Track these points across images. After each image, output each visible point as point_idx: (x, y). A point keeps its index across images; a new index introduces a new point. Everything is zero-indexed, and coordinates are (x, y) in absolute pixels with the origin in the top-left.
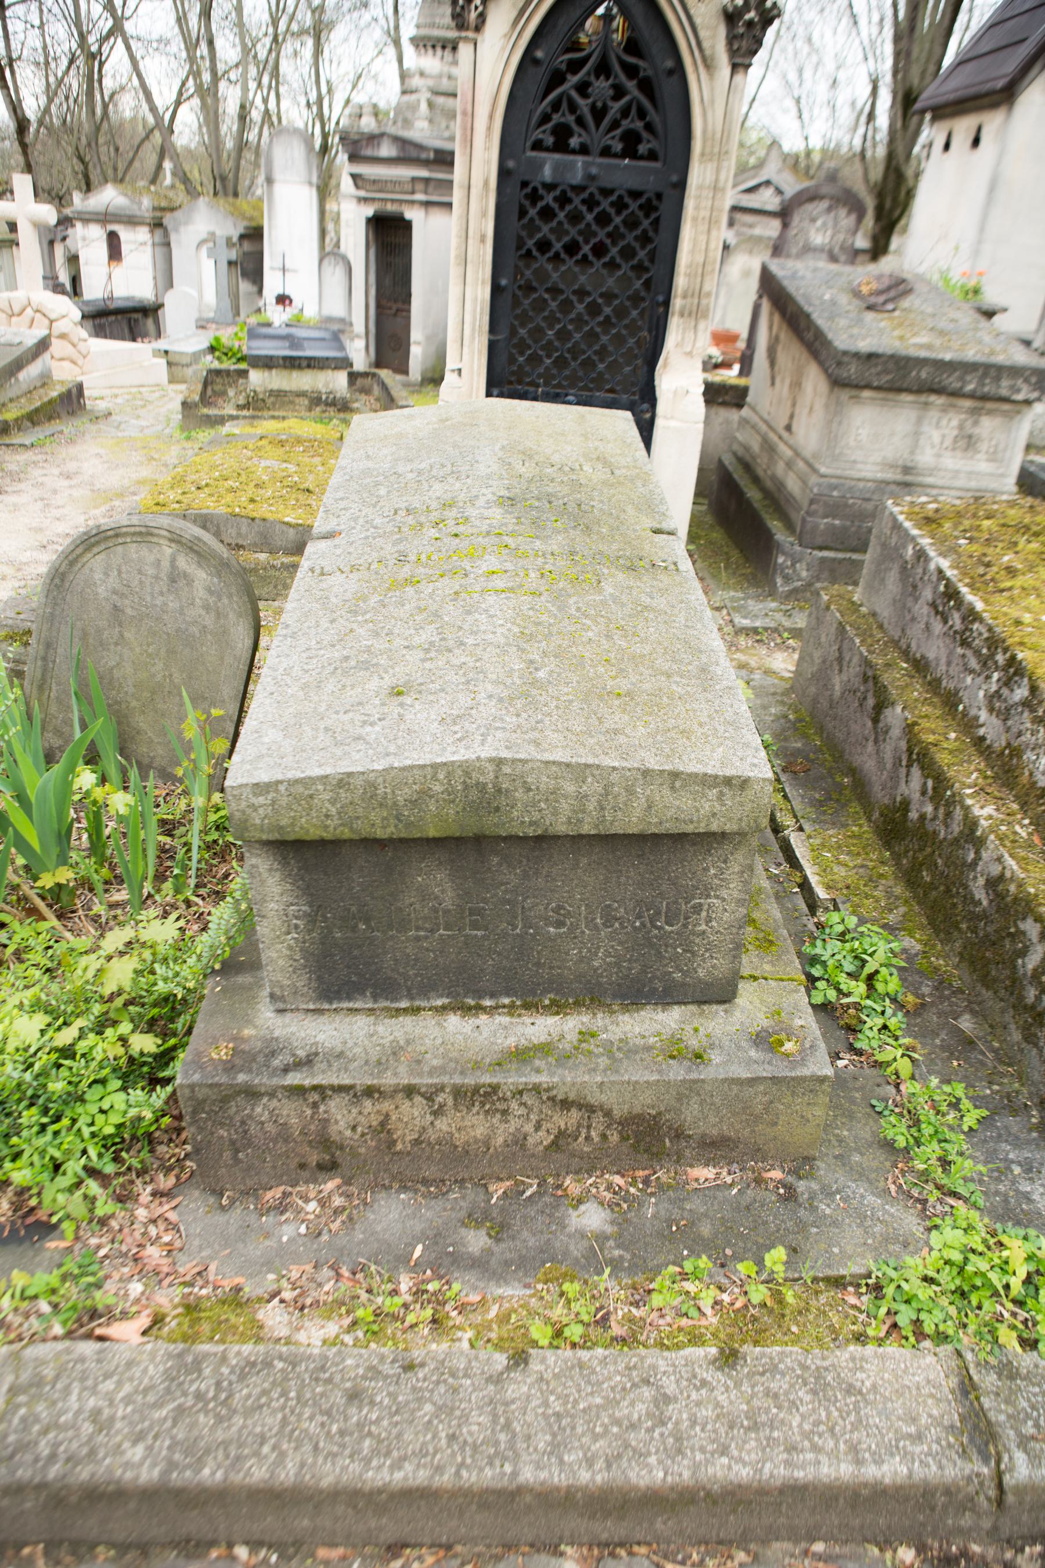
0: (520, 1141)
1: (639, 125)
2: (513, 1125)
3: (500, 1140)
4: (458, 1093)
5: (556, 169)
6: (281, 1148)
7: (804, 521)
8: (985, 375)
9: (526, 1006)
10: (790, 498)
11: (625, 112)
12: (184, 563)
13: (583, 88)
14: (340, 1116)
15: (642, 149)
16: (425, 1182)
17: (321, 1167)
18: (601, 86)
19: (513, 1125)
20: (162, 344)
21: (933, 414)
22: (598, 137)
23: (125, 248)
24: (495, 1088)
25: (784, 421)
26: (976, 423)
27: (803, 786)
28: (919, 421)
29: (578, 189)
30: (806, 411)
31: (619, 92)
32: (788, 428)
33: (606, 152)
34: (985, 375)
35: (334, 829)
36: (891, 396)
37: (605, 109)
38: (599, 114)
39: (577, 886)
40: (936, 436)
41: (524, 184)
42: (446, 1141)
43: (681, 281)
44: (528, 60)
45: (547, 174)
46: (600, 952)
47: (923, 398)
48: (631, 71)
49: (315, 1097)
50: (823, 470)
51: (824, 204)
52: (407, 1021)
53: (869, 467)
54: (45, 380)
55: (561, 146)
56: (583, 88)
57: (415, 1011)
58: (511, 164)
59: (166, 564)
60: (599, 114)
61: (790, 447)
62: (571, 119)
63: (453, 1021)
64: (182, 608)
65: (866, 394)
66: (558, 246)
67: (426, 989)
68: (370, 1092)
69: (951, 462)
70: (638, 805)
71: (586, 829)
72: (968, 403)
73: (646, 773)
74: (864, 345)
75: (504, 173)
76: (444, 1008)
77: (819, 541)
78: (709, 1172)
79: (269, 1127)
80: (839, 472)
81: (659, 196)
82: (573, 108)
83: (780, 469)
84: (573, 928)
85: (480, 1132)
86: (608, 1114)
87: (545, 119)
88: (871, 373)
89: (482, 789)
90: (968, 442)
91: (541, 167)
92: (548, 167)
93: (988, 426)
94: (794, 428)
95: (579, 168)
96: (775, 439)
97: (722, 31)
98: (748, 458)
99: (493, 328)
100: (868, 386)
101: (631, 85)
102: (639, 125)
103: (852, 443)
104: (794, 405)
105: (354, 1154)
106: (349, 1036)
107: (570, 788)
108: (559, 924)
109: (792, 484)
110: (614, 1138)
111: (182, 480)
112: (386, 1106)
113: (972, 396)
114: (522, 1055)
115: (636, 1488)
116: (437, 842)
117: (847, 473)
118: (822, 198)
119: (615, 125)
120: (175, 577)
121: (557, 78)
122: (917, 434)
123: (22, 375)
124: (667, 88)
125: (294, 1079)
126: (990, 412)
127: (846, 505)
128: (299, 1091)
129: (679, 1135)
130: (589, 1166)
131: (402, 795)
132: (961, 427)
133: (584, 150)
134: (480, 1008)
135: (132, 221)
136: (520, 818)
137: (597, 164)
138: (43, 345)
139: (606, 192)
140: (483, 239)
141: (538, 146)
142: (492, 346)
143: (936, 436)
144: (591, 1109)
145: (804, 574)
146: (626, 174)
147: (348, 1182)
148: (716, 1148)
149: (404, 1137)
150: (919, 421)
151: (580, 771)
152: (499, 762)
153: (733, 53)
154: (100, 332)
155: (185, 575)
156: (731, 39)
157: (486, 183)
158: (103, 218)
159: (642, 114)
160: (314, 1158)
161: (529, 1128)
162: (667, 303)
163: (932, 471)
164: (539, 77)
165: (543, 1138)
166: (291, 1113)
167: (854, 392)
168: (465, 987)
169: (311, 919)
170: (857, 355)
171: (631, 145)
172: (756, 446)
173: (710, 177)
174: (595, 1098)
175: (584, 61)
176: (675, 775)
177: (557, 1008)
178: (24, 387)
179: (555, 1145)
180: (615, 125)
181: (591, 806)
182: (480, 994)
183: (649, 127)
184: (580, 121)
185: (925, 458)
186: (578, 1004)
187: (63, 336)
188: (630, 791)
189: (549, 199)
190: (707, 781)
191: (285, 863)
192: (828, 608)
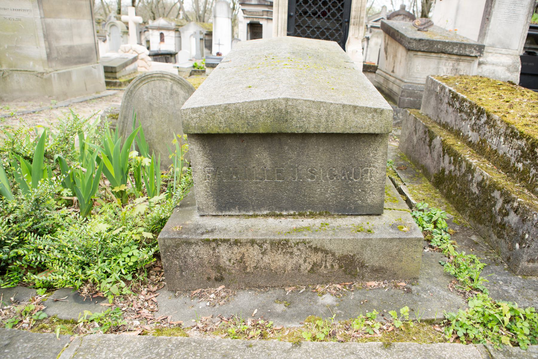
0: (298, 268)
2: (296, 259)
3: (289, 268)
4: (272, 243)
6: (200, 270)
7: (400, 99)
8: (460, 47)
9: (300, 215)
10: (395, 94)
12: (176, 88)
14: (225, 255)
16: (259, 287)
17: (216, 279)
21: (443, 61)
23: (165, 38)
24: (287, 241)
25: (392, 69)
26: (458, 64)
27: (405, 173)
28: (438, 63)
30: (398, 64)
32: (393, 72)
34: (460, 47)
36: (428, 54)
42: (267, 268)
43: (353, 13)
47: (439, 55)
49: (214, 245)
50: (406, 80)
52: (253, 220)
53: (422, 80)
54: (135, 71)
57: (256, 216)
59: (169, 88)
61: (394, 77)
63: (271, 220)
64: (174, 104)
65: (419, 53)
66: (310, 12)
67: (260, 207)
68: (237, 242)
72: (455, 57)
76: (267, 216)
77: (406, 105)
78: (374, 284)
79: (195, 259)
80: (411, 81)
83: (391, 85)
84: (318, 178)
85: (281, 263)
86: (333, 255)
94: (395, 71)
96: (389, 76)
103: (415, 71)
104: (394, 63)
105: (230, 274)
106: (230, 225)
108: (312, 178)
109: (395, 89)
110: (336, 267)
112: (243, 250)
113: (456, 55)
114: (298, 230)
117: (414, 82)
120: (172, 93)
123: (128, 68)
125: (205, 237)
127: (415, 93)
128: (207, 242)
129: (363, 266)
130: (326, 280)
132: (453, 66)
134: (281, 215)
135: (168, 29)
138: (135, 59)
144: (326, 252)
145: (401, 117)
147: (228, 287)
148: (379, 272)
149: (251, 264)
150: (438, 63)
154: (155, 60)
155: (176, 92)
158: (159, 28)
160: (213, 275)
161: (301, 261)
165: (306, 267)
166: (204, 252)
167: (415, 53)
168: (276, 206)
169: (215, 173)
170: (415, 40)
172: (382, 81)
174: (329, 247)
177: (312, 215)
178: (128, 72)
179: (312, 270)
182: (281, 209)
186: (321, 214)
187: (142, 59)
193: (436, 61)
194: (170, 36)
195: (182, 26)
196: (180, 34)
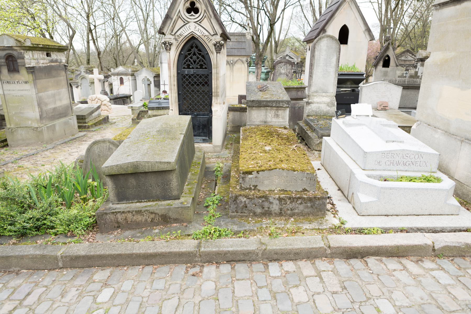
0: (146, 220)
1: (202, 63)
2: (145, 217)
3: (143, 220)
4: (136, 212)
5: (188, 72)
6: (111, 224)
8: (277, 103)
9: (149, 201)
11: (200, 61)
13: (191, 58)
14: (120, 217)
15: (203, 67)
16: (133, 229)
17: (117, 227)
18: (194, 57)
19: (145, 217)
20: (131, 105)
21: (269, 111)
22: (194, 66)
24: (141, 210)
26: (278, 112)
28: (266, 112)
29: (192, 75)
31: (198, 58)
33: (197, 68)
34: (277, 103)
35: (117, 173)
37: (196, 61)
38: (195, 62)
39: (152, 180)
40: (270, 115)
41: (182, 75)
42: (135, 221)
43: (213, 90)
44: (180, 54)
45: (186, 73)
46: (157, 191)
47: (266, 108)
48: (200, 54)
49: (115, 214)
51: (284, 64)
52: (131, 204)
54: (99, 115)
55: (189, 68)
56: (191, 58)
57: (132, 203)
58: (179, 71)
60: (195, 62)
62: (190, 63)
63: (138, 204)
65: (254, 108)
67: (134, 199)
68: (123, 212)
69: (274, 120)
70: (157, 166)
71: (150, 171)
72: (275, 108)
73: (157, 162)
74: (252, 99)
75: (178, 73)
76: (137, 202)
78: (175, 225)
79: (109, 220)
81: (208, 75)
82: (190, 61)
84: (153, 187)
85: (140, 219)
86: (158, 215)
87: (185, 63)
88: (254, 104)
89: (135, 165)
90: (277, 116)
91: (185, 71)
92: (186, 71)
93: (280, 112)
95: (192, 71)
97: (214, 47)
99: (179, 101)
100: (253, 107)
101: (200, 56)
102: (202, 63)
105: (122, 224)
106: (122, 206)
107: (147, 165)
108: (151, 187)
110: (160, 219)
111: (121, 134)
112: (126, 215)
113: (275, 107)
114: (146, 207)
115: (148, 253)
116: (132, 174)
118: (282, 62)
119: (198, 63)
121: (186, 56)
122: (266, 115)
124: (206, 57)
125: (112, 211)
126: (280, 110)
128: (113, 213)
129: (170, 218)
130: (157, 225)
131: (125, 167)
132: (275, 113)
133: (193, 68)
134: (142, 202)
136: (141, 170)
137: (195, 70)
139: (198, 75)
140: (174, 85)
141: (184, 68)
142: (179, 105)
143: (270, 115)
144: (155, 214)
146: (201, 72)
147: (122, 230)
148: (176, 220)
149: (129, 220)
150: (266, 112)
151: (148, 162)
152: (137, 162)
153: (216, 51)
156: (215, 48)
157: (174, 75)
159: (203, 61)
160: (116, 225)
161: (147, 218)
162: (212, 94)
163: (271, 122)
164: (182, 57)
165: (149, 220)
166: (112, 217)
168: (139, 199)
169: (116, 188)
170: (250, 101)
171: (201, 67)
173: (215, 71)
174: (156, 212)
175: (191, 53)
176: (161, 162)
177: (153, 201)
178: (94, 117)
179: (152, 221)
180: (198, 63)
181: (150, 167)
182: (142, 199)
183: (204, 63)
184: (191, 63)
185: (269, 119)
186: (156, 200)
188: (155, 165)
189: (187, 77)
190: (165, 163)
191: (111, 179)
193: (264, 111)
194: (128, 80)
195: (137, 71)
196: (135, 77)
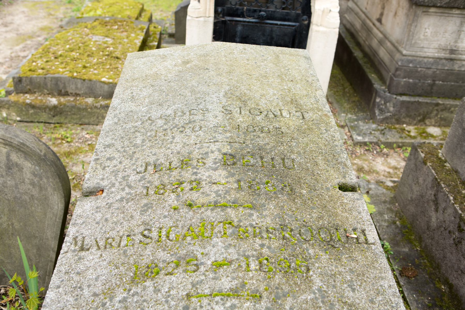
7: (391, 79)
10: (381, 62)
12: (14, 157)
25: (378, 16)
27: (416, 291)
30: (391, 14)
32: (380, 20)
36: (447, 11)
50: (404, 52)
53: (431, 50)
61: (381, 32)
64: (16, 185)
65: (432, 10)
77: (400, 90)
80: (414, 53)
83: (375, 43)
94: (383, 21)
96: (371, 25)
98: (352, 30)
100: (435, 6)
103: (422, 37)
104: (383, 8)
109: (383, 53)
111: (46, 51)
117: (419, 54)
120: (10, 166)
127: (417, 71)
145: (392, 109)
155: (17, 165)
167: (425, 9)
172: (358, 25)
192: (425, 163)
193: (458, 21)
